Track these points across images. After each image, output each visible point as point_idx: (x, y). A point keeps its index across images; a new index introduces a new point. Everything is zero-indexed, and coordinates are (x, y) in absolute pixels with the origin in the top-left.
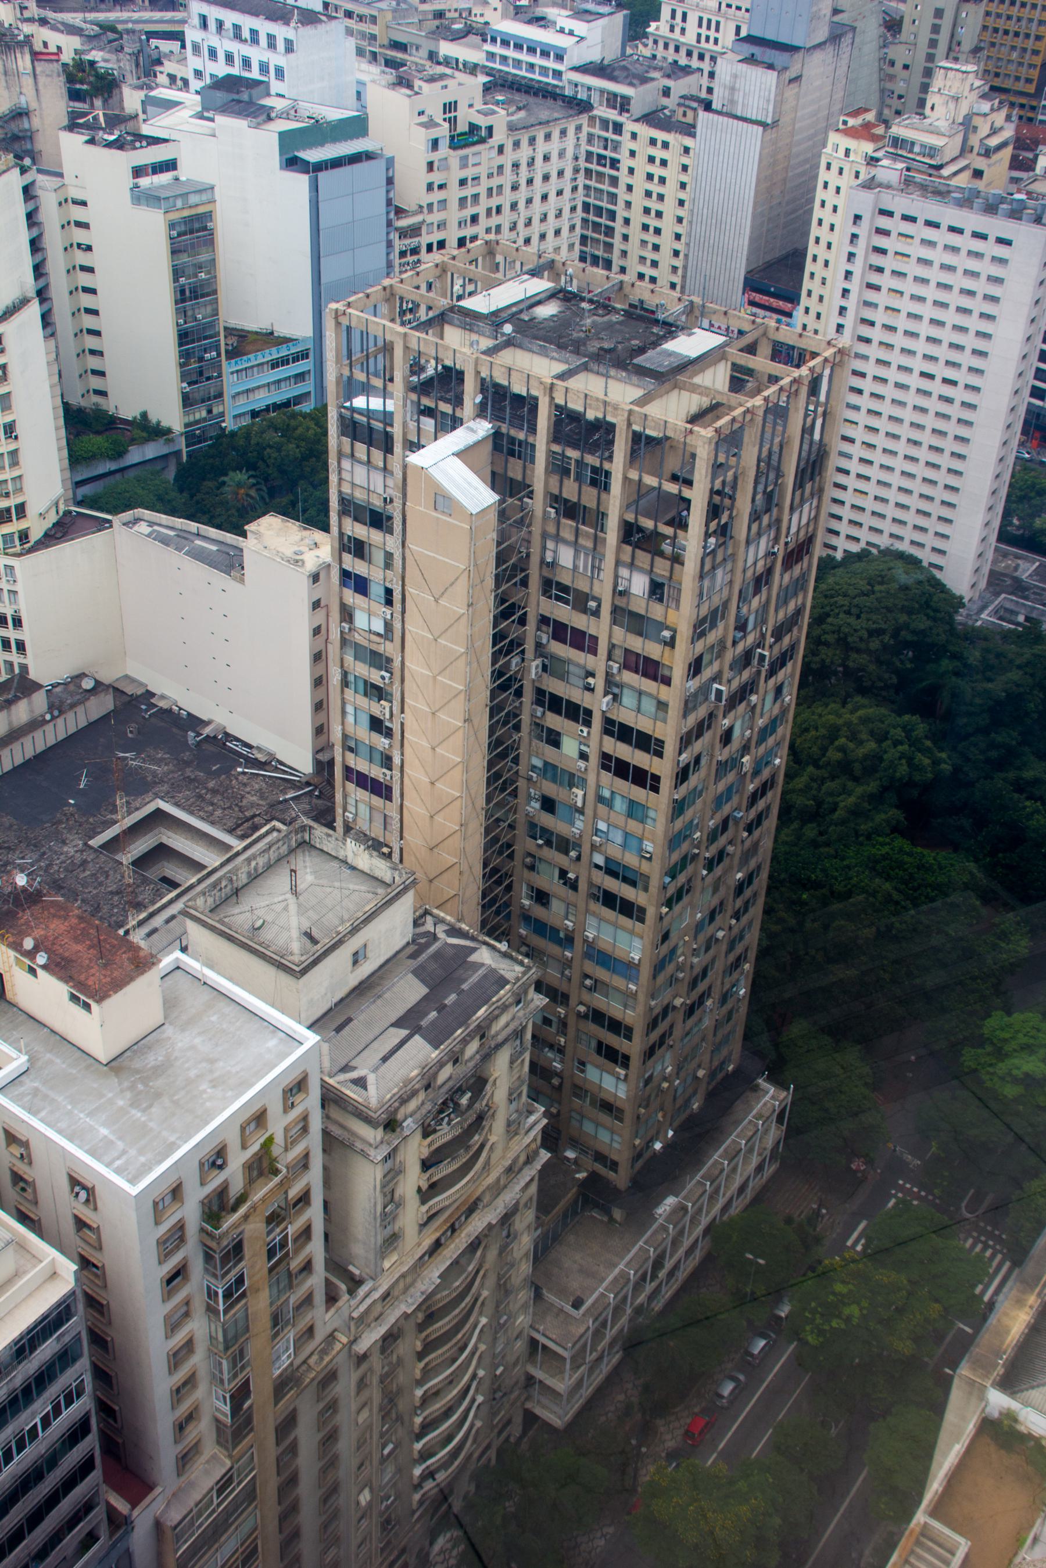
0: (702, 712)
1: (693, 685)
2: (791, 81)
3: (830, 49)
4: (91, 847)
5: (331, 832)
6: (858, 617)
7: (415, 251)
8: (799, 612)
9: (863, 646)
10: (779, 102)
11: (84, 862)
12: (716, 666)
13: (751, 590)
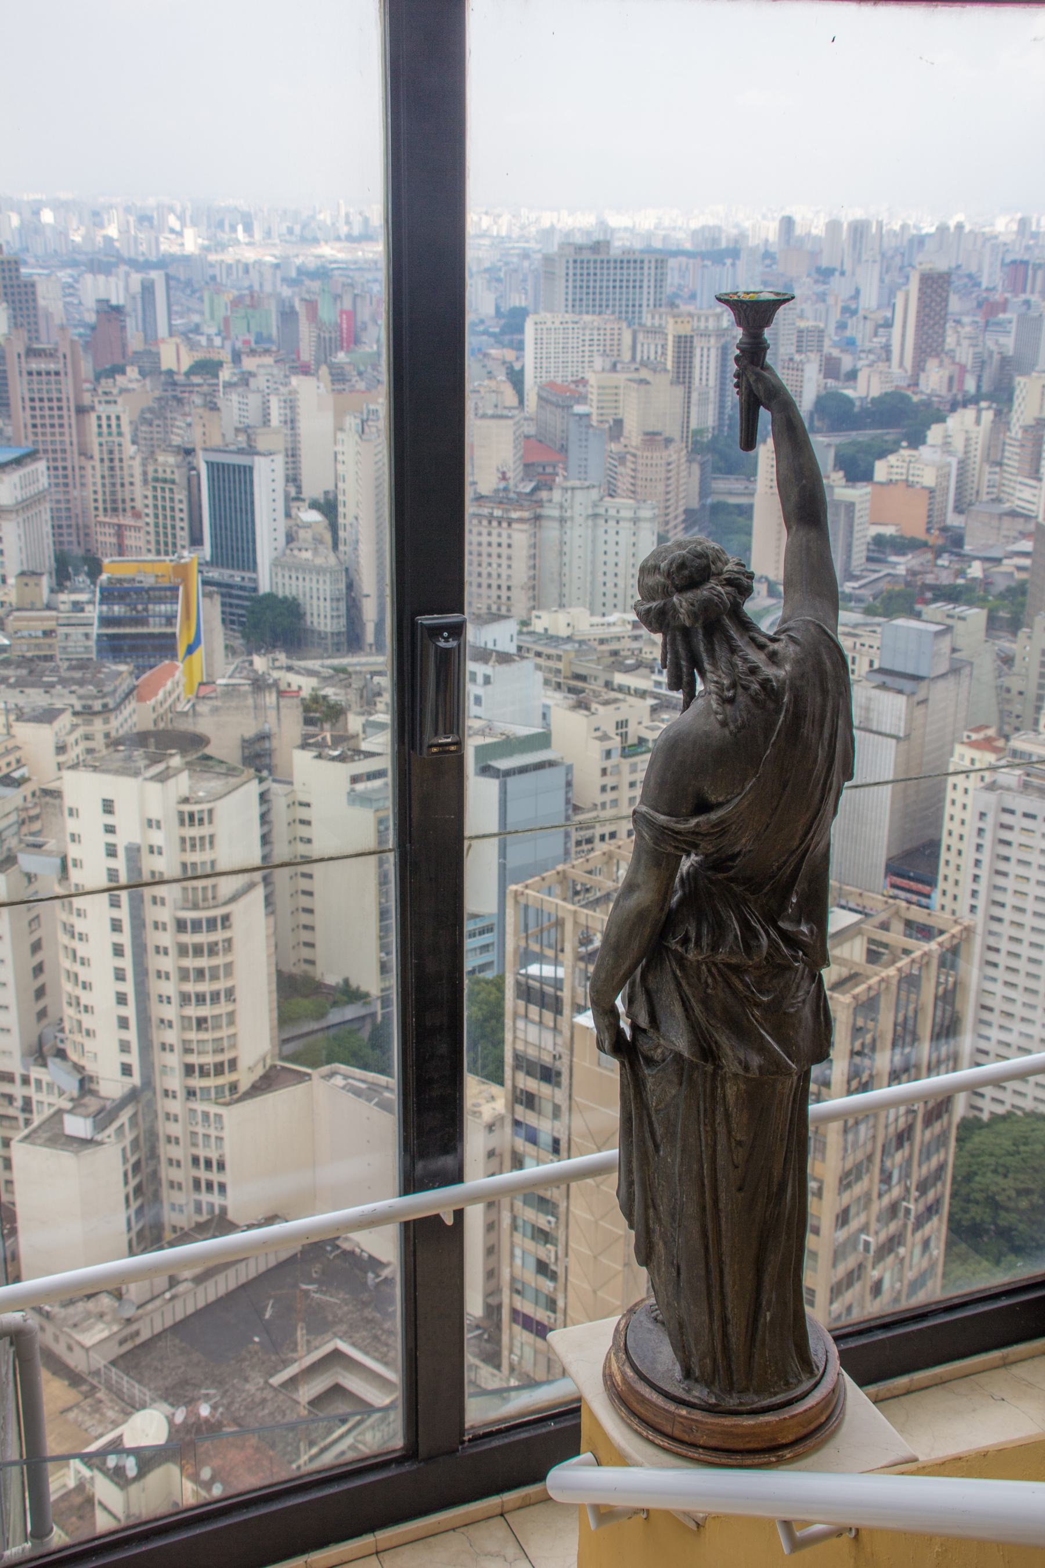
0: (850, 1262)
1: (842, 1235)
2: (919, 703)
3: (951, 679)
4: (271, 1386)
5: (496, 1372)
6: (1005, 1176)
7: (589, 841)
8: (941, 1167)
9: (1012, 1205)
10: (910, 719)
11: (264, 1401)
12: (863, 1218)
13: (894, 1144)
